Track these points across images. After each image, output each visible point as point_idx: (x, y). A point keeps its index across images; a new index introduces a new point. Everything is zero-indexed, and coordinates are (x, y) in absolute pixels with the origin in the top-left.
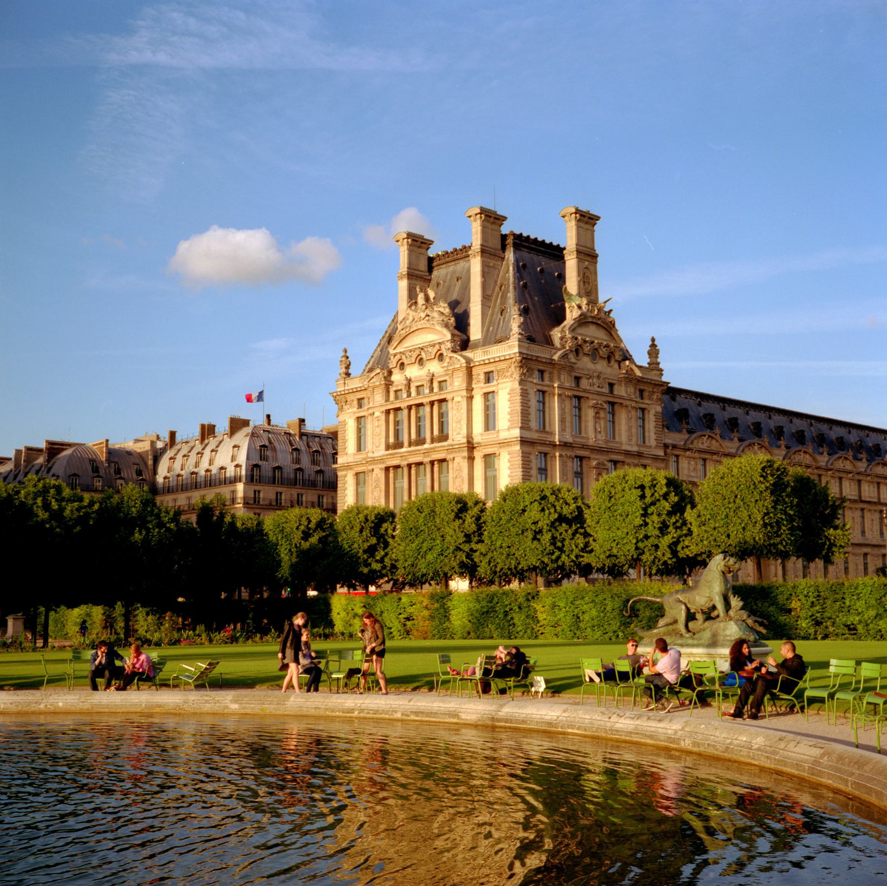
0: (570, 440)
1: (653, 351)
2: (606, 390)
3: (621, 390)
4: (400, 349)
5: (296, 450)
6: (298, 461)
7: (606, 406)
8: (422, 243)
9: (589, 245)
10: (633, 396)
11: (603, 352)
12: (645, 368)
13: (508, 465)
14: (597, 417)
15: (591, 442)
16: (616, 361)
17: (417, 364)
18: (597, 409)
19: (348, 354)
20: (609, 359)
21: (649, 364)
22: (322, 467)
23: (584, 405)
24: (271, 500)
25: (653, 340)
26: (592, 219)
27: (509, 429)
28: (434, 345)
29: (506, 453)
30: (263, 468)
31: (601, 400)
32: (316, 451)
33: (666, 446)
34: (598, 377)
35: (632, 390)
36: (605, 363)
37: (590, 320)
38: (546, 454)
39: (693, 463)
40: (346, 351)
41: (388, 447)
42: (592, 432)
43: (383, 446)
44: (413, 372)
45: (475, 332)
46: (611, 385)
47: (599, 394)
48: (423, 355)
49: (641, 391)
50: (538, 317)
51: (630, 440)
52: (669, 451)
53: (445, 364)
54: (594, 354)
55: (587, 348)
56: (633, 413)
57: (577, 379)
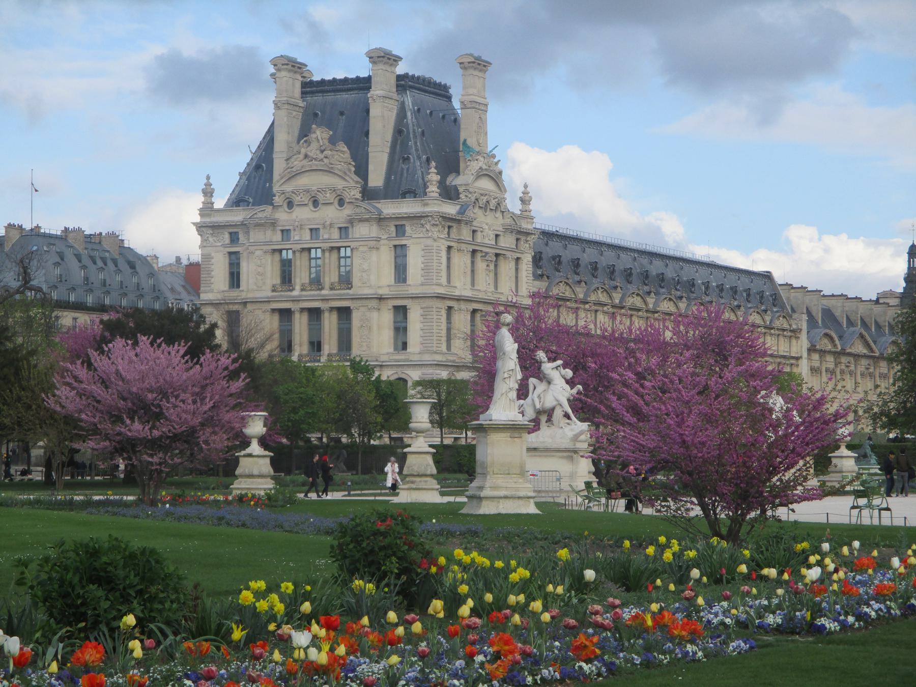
40: (208, 178)
44: (303, 214)
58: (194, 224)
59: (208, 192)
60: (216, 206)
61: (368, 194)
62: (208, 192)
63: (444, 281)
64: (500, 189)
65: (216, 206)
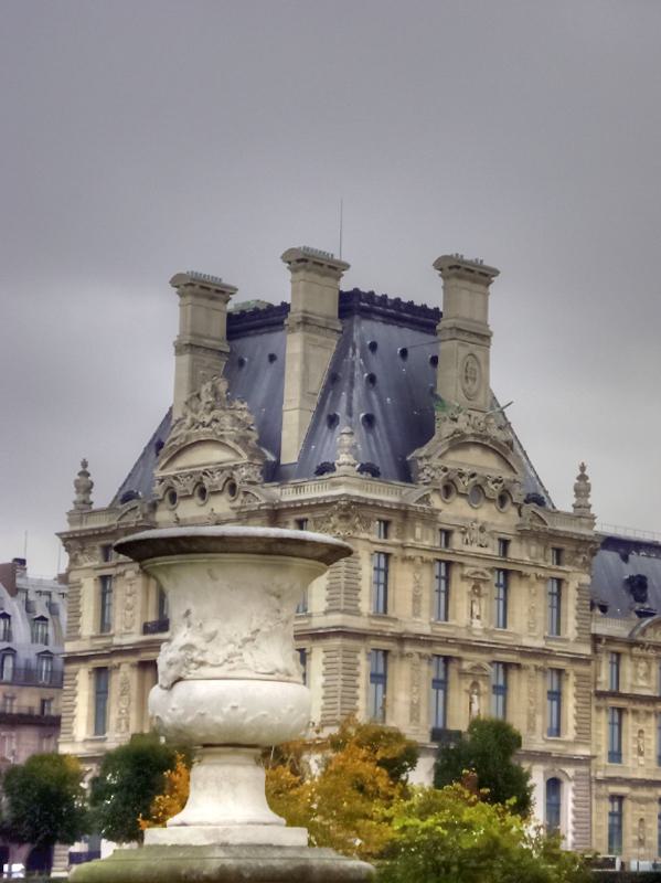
0: (426, 630)
1: (582, 488)
2: (493, 550)
3: (516, 551)
4: (170, 472)
7: (493, 578)
8: (217, 291)
9: (477, 317)
10: (541, 562)
11: (493, 490)
12: (568, 515)
13: (323, 668)
14: (476, 591)
15: (463, 635)
16: (514, 504)
17: (197, 499)
18: (477, 584)
19: (88, 469)
20: (503, 499)
21: (574, 506)
22: (51, 647)
23: (456, 573)
25: (583, 468)
26: (486, 275)
27: (326, 612)
28: (221, 470)
29: (321, 649)
31: (482, 566)
32: (42, 618)
33: (596, 639)
34: (482, 529)
35: (541, 550)
36: (493, 507)
37: (471, 439)
38: (386, 653)
39: (643, 665)
41: (146, 629)
42: (470, 616)
43: (137, 627)
45: (290, 453)
46: (505, 543)
47: (487, 558)
48: (207, 482)
49: (559, 552)
50: (389, 433)
51: (531, 629)
52: (600, 646)
53: (238, 503)
54: (478, 493)
55: (465, 485)
56: (541, 587)
57: (447, 534)
58: (59, 535)
59: (85, 486)
60: (94, 507)
61: (274, 473)
62: (85, 486)
63: (366, 605)
64: (511, 468)
65: (94, 507)
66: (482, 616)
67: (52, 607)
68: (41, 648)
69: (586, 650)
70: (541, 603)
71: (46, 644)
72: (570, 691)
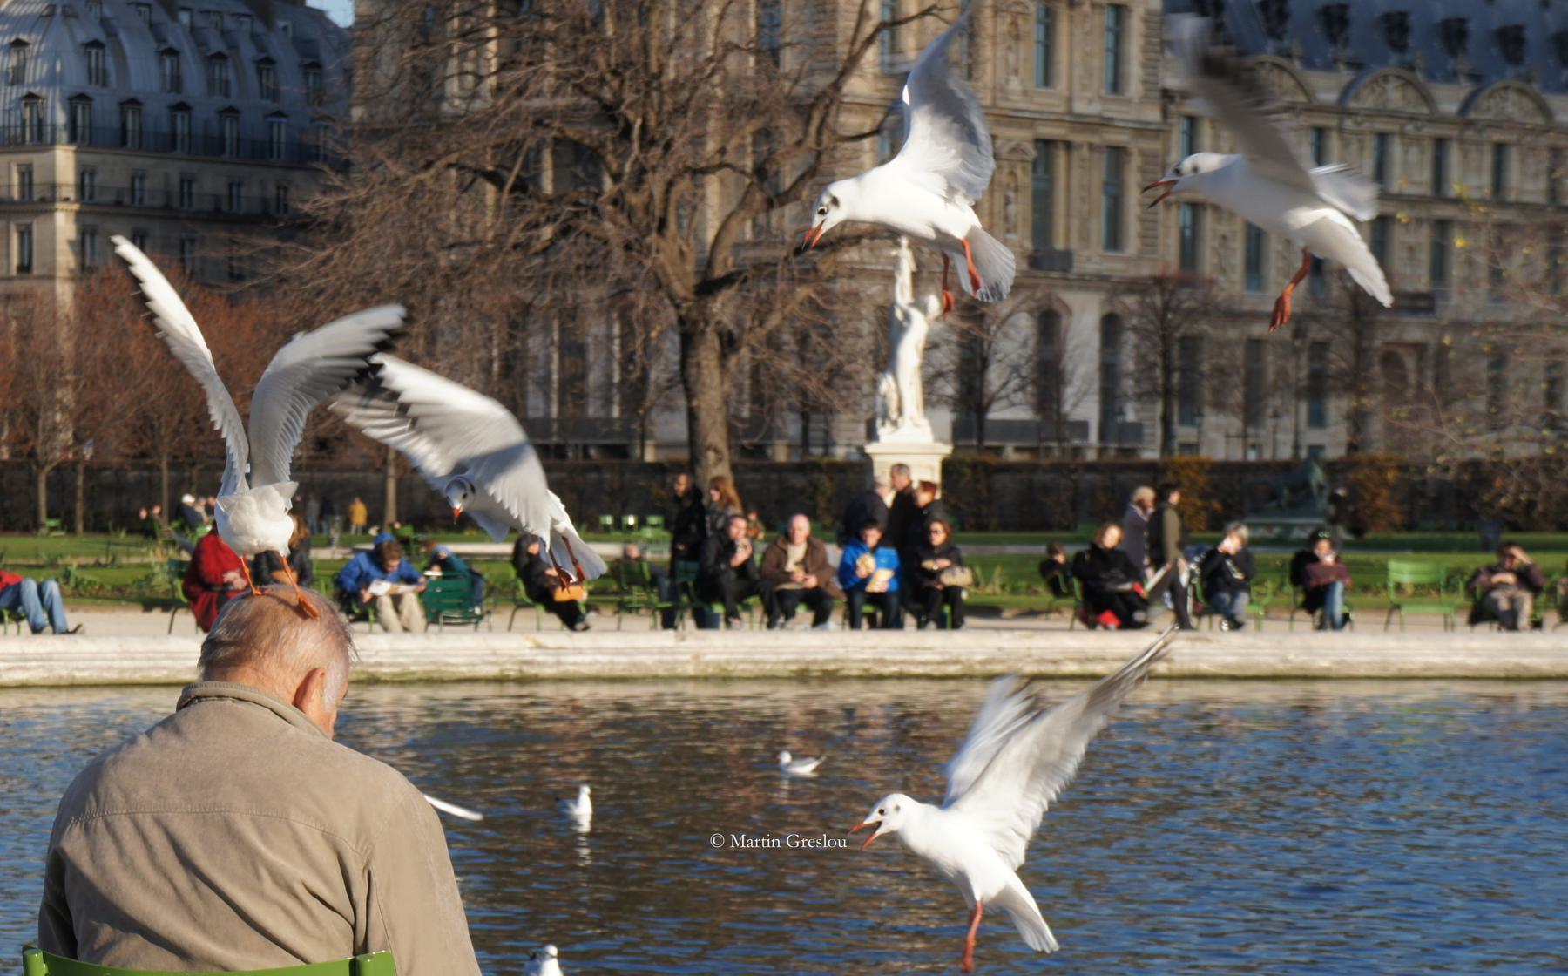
5: (172, 52)
6: (176, 82)
22: (233, 101)
24: (120, 191)
30: (97, 104)
32: (220, 56)
33: (1167, 95)
52: (1172, 108)
66: (1021, 69)
67: (224, 33)
68: (219, 101)
69: (1153, 115)
70: (1099, 44)
71: (227, 95)
72: (1133, 179)
